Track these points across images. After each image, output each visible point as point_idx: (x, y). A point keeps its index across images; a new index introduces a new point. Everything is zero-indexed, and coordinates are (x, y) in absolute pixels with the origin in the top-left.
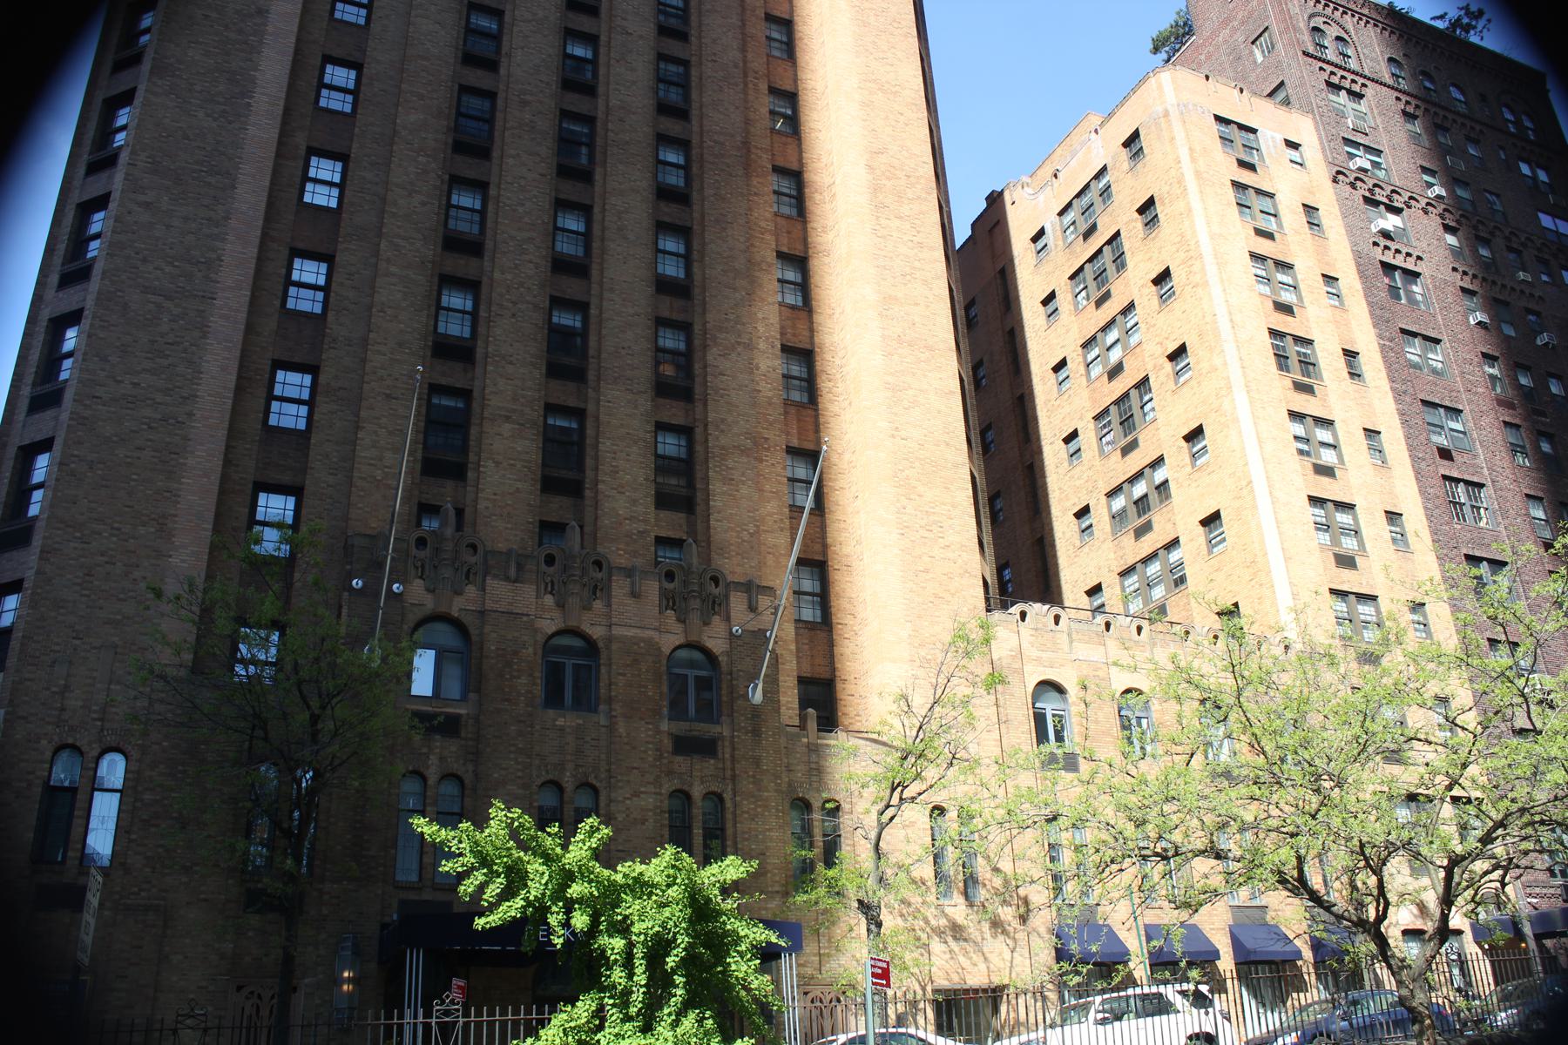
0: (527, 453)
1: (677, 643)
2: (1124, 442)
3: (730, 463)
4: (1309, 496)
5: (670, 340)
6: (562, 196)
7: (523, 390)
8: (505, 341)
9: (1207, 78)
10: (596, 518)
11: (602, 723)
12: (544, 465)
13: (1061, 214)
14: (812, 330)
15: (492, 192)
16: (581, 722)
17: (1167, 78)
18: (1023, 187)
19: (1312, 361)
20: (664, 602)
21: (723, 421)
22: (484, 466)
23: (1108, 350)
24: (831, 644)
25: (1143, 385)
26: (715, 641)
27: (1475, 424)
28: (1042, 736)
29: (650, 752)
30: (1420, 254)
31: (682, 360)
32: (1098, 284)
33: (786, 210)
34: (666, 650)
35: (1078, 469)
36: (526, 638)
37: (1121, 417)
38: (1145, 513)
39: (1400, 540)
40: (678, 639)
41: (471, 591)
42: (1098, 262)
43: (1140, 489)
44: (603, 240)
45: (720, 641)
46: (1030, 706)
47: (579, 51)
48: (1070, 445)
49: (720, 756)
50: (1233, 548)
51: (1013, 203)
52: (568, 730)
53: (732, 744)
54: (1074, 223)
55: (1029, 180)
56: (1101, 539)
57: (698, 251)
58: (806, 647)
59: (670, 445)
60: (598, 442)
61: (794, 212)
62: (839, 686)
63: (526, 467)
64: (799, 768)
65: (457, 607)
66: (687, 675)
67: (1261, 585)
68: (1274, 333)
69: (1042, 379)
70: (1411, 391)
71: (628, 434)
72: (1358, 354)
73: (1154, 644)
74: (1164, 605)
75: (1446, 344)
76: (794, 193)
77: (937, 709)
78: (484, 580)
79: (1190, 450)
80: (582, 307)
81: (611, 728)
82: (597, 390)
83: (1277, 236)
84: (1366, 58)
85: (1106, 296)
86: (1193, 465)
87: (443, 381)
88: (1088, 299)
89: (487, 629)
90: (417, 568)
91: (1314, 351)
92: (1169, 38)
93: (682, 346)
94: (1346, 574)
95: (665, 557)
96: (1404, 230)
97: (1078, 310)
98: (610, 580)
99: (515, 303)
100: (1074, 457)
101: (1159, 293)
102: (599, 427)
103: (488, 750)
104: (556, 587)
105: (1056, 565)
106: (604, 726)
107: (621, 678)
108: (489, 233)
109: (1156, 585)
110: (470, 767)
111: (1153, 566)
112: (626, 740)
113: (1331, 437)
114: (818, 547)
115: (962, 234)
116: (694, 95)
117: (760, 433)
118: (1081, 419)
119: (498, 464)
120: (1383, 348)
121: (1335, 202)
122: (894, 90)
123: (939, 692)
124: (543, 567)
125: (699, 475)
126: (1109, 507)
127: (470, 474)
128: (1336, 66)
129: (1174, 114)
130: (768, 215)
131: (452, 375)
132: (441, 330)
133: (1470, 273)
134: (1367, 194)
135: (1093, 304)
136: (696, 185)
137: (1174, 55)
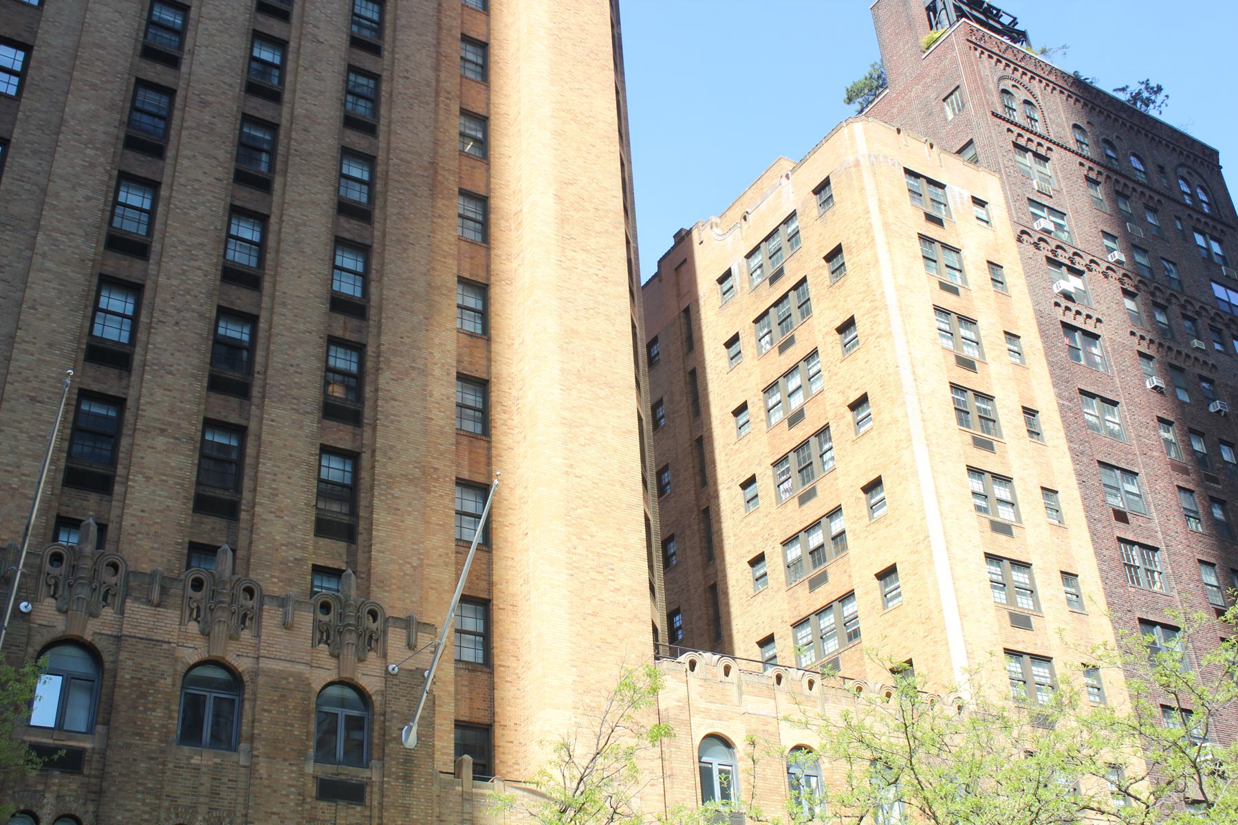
0: (181, 469)
1: (329, 680)
2: (802, 490)
3: (396, 492)
4: (985, 553)
5: (342, 360)
6: (237, 203)
7: (181, 402)
8: (166, 350)
9: (899, 131)
10: (251, 542)
11: (241, 763)
12: (199, 483)
13: (749, 256)
14: (489, 360)
15: (164, 192)
16: (218, 761)
17: (859, 127)
18: (712, 228)
19: (992, 417)
20: (318, 635)
21: (392, 448)
22: (134, 481)
23: (789, 396)
24: (492, 687)
25: (824, 432)
26: (370, 678)
27: (1150, 487)
28: (707, 793)
29: (292, 797)
30: (1100, 317)
31: (352, 382)
32: (782, 329)
33: (470, 235)
34: (317, 687)
35: (754, 515)
36: (165, 667)
37: (800, 465)
38: (820, 564)
39: (1075, 601)
40: (332, 676)
41: (108, 613)
42: (783, 307)
43: (816, 539)
44: (278, 252)
45: (374, 679)
46: (696, 760)
47: (267, 55)
48: (748, 490)
49: (368, 803)
50: (909, 603)
51: (702, 242)
52: (204, 769)
53: (381, 790)
54: (761, 266)
55: (718, 221)
56: (776, 588)
57: (377, 271)
58: (465, 689)
59: (335, 470)
60: (258, 463)
61: (479, 238)
62: (498, 731)
63: (178, 484)
64: (451, 818)
65: (91, 630)
66: (337, 714)
67: (936, 642)
68: (955, 387)
69: (722, 422)
70: (1088, 451)
71: (291, 455)
72: (1038, 412)
73: (826, 700)
74: (837, 658)
75: (1123, 406)
76: (480, 218)
77: (600, 760)
78: (123, 603)
79: (868, 502)
80: (250, 320)
81: (251, 769)
82: (261, 407)
83: (961, 291)
84: (1052, 122)
85: (790, 342)
87: (95, 387)
88: (772, 344)
89: (123, 656)
90: (50, 586)
91: (994, 407)
92: (861, 90)
93: (354, 368)
94: (1021, 634)
95: (321, 587)
96: (1085, 292)
97: (761, 355)
98: (261, 609)
99: (179, 311)
100: (751, 503)
101: (842, 341)
102: (259, 446)
103: (113, 789)
104: (202, 614)
105: (728, 613)
106: (245, 767)
107: (266, 714)
108: (157, 235)
109: (830, 637)
110: (91, 808)
111: (826, 619)
112: (266, 783)
113: (1008, 494)
114: (483, 584)
115: (648, 270)
116: (383, 111)
117: (430, 462)
118: (759, 464)
119: (148, 478)
120: (1061, 407)
121: (1019, 261)
122: (587, 121)
123: (602, 742)
124: (190, 591)
125: (363, 502)
126: (785, 556)
127: (118, 488)
128: (1023, 128)
129: (865, 164)
130: (452, 239)
131: (105, 381)
132: (97, 332)
133: (1147, 338)
134: (1050, 255)
135: (776, 349)
136: (379, 202)
137: (867, 106)
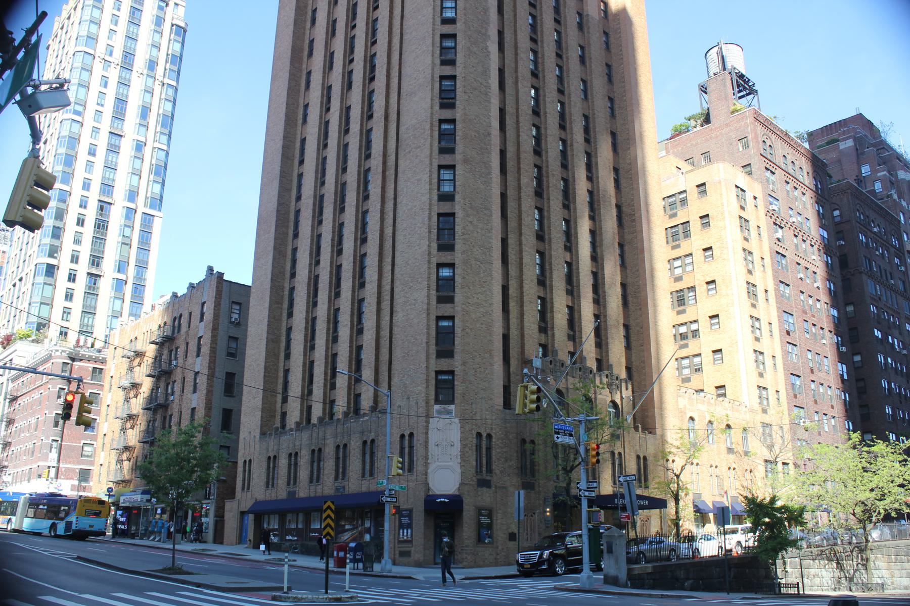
25: (692, 289)
75: (791, 287)
85: (678, 246)
86: (711, 329)
94: (761, 379)
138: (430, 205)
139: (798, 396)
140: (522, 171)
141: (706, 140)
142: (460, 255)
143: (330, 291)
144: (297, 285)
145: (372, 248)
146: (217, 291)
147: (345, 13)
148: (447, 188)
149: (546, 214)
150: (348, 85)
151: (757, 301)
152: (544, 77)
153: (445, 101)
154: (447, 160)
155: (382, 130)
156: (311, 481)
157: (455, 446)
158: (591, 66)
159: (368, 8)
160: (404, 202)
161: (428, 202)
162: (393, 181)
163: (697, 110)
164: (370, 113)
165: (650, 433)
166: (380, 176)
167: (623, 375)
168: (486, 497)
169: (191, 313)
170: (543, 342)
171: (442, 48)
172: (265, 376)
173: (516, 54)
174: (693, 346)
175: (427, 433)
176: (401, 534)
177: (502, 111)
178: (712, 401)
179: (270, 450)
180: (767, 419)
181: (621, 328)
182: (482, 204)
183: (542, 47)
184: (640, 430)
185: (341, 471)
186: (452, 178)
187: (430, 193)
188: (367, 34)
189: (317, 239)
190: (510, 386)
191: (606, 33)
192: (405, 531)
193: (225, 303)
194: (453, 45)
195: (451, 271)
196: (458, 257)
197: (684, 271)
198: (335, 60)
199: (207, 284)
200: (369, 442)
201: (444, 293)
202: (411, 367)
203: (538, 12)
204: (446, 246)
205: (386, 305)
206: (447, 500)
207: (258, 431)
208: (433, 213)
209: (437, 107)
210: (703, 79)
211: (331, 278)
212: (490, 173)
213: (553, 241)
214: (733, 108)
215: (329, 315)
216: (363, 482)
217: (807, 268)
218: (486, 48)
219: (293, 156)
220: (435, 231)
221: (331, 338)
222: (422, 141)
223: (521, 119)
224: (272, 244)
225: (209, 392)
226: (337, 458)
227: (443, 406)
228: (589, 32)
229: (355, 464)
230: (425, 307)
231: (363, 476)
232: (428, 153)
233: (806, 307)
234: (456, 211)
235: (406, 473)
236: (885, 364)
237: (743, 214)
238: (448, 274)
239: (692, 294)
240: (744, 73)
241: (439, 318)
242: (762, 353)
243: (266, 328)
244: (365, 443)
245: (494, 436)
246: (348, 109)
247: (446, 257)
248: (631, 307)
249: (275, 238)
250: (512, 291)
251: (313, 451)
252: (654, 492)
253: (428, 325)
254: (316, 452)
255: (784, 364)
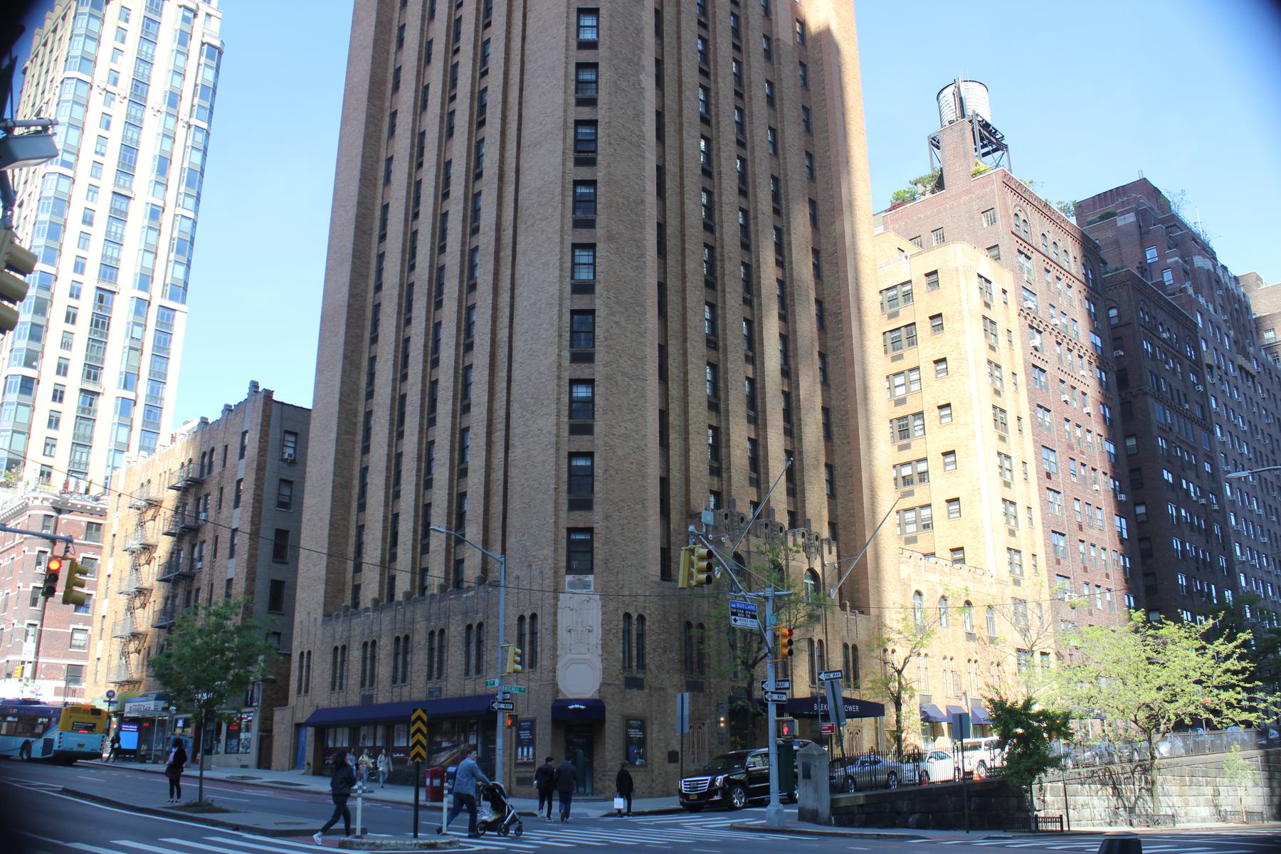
25: (919, 415)
75: (1052, 412)
85: (900, 357)
138: (561, 298)
139: (1062, 561)
140: (687, 252)
141: (939, 212)
142: (601, 368)
143: (422, 417)
144: (375, 408)
145: (480, 358)
146: (263, 416)
147: (445, 31)
148: (584, 275)
149: (720, 312)
150: (448, 131)
151: (1006, 431)
152: (718, 123)
153: (582, 155)
154: (584, 236)
155: (495, 194)
156: (394, 681)
157: (595, 632)
158: (782, 110)
159: (477, 26)
160: (525, 294)
161: (558, 294)
162: (509, 265)
163: (926, 171)
164: (478, 171)
165: (862, 613)
166: (492, 258)
167: (825, 533)
168: (637, 702)
169: (226, 447)
170: (715, 488)
171: (578, 82)
172: (330, 535)
173: (680, 92)
174: (920, 494)
175: (555, 614)
176: (520, 753)
177: (661, 170)
178: (946, 569)
179: (337, 637)
180: (1020, 593)
181: (823, 469)
182: (631, 298)
183: (716, 82)
184: (848, 608)
185: (436, 668)
186: (591, 261)
187: (561, 282)
188: (474, 60)
189: (404, 345)
190: (669, 549)
191: (803, 65)
192: (525, 750)
193: (275, 433)
194: (594, 77)
195: (590, 390)
196: (598, 370)
197: (908, 391)
198: (430, 97)
199: (249, 406)
200: (475, 627)
201: (578, 421)
202: (534, 522)
203: (711, 34)
204: (582, 356)
205: (499, 436)
206: (583, 707)
207: (320, 612)
208: (564, 310)
209: (571, 164)
210: (934, 129)
211: (423, 399)
212: (643, 255)
213: (730, 349)
214: (974, 169)
215: (420, 450)
216: (467, 681)
217: (1073, 388)
218: (639, 82)
219: (372, 229)
220: (568, 335)
221: (422, 482)
222: (550, 210)
223: (687, 181)
224: (341, 351)
225: (252, 557)
226: (431, 649)
227: (577, 577)
228: (779, 63)
229: (455, 657)
230: (553, 439)
231: (467, 673)
232: (558, 227)
233: (1073, 441)
234: (597, 308)
235: (527, 670)
236: (1177, 517)
237: (988, 314)
238: (584, 395)
239: (919, 422)
240: (989, 122)
241: (572, 455)
242: (1013, 503)
243: (331, 469)
244: (469, 627)
245: (647, 618)
246: (448, 164)
247: (582, 371)
248: (836, 441)
249: (346, 343)
250: (674, 419)
251: (397, 639)
252: (866, 693)
253: (557, 465)
254: (402, 640)
255: (1043, 519)
